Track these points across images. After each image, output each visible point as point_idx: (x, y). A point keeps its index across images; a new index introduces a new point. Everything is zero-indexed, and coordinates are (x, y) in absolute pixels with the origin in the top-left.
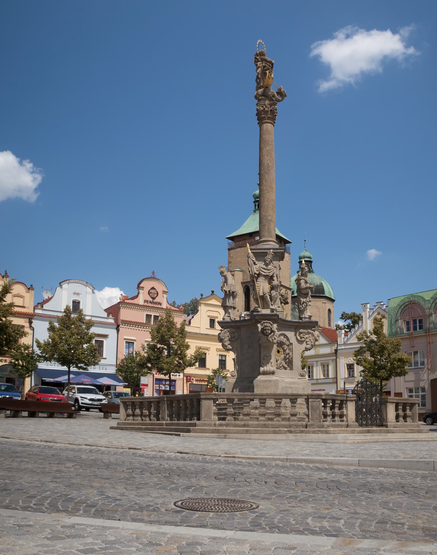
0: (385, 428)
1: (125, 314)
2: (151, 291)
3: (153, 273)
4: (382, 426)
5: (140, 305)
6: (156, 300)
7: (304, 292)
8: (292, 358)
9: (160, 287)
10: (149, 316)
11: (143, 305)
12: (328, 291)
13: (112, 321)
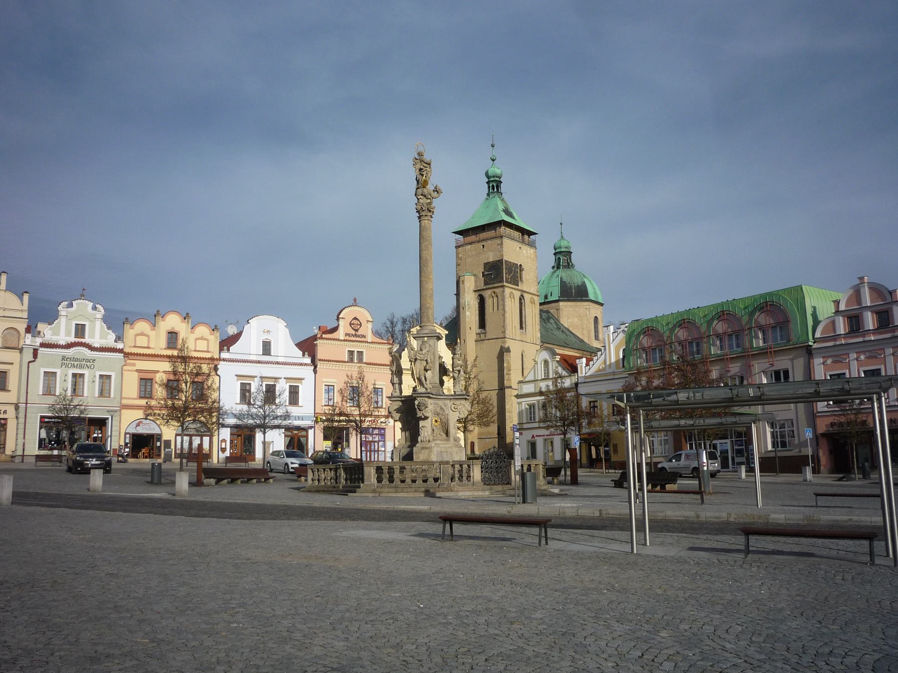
1: (324, 348)
3: (355, 300)
6: (359, 333)
11: (344, 340)
12: (593, 290)
13: (308, 360)
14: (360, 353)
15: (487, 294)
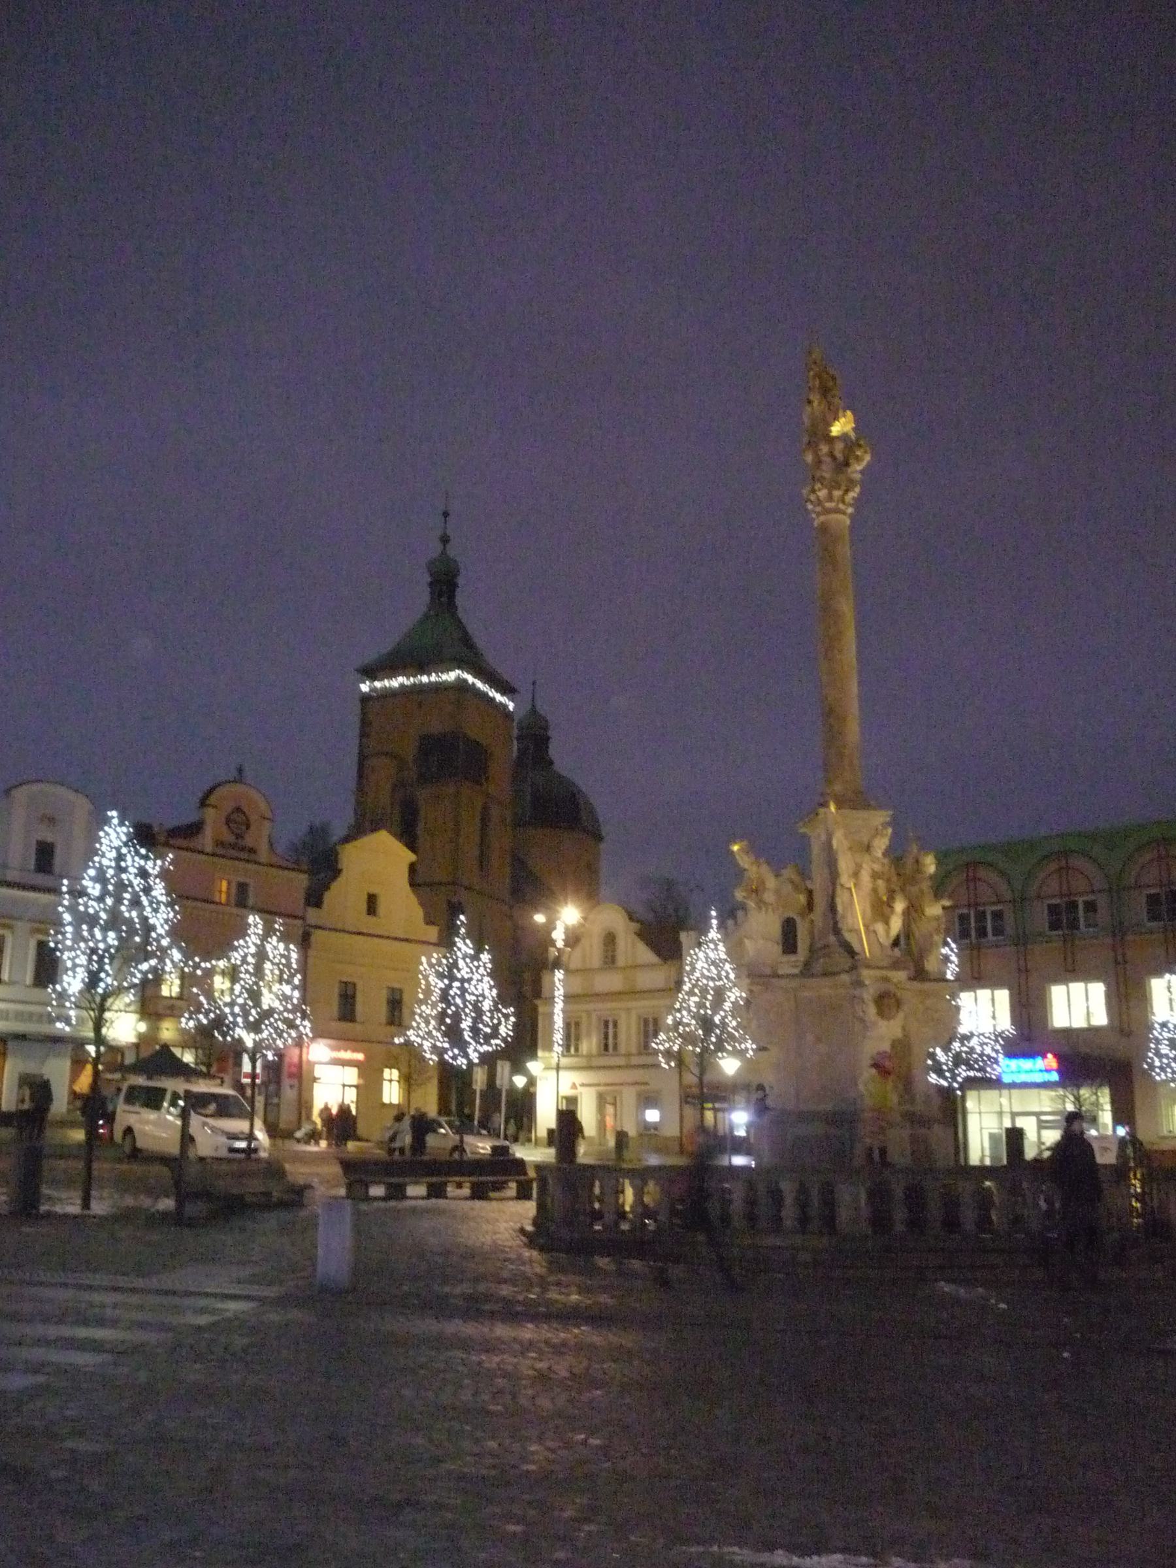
3: (240, 770)
6: (249, 841)
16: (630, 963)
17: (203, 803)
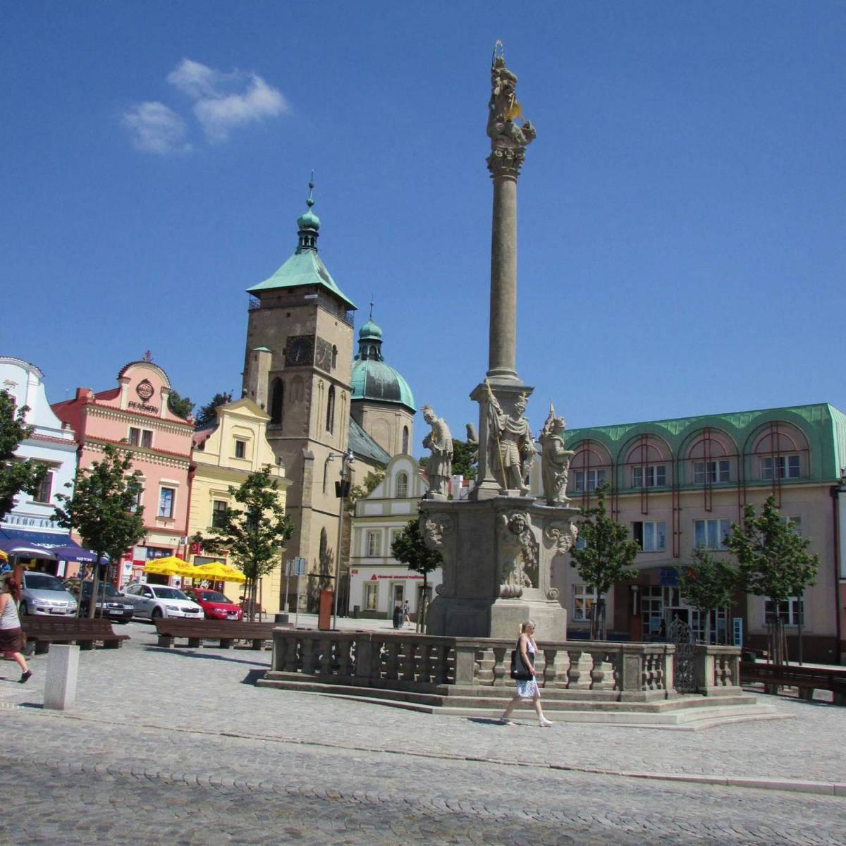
0: (700, 698)
2: (141, 386)
3: (148, 353)
4: (697, 692)
5: (122, 411)
7: (561, 460)
8: (537, 568)
9: (158, 381)
10: (135, 432)
12: (407, 396)
14: (148, 435)
15: (287, 378)
16: (415, 495)
17: (120, 377)
